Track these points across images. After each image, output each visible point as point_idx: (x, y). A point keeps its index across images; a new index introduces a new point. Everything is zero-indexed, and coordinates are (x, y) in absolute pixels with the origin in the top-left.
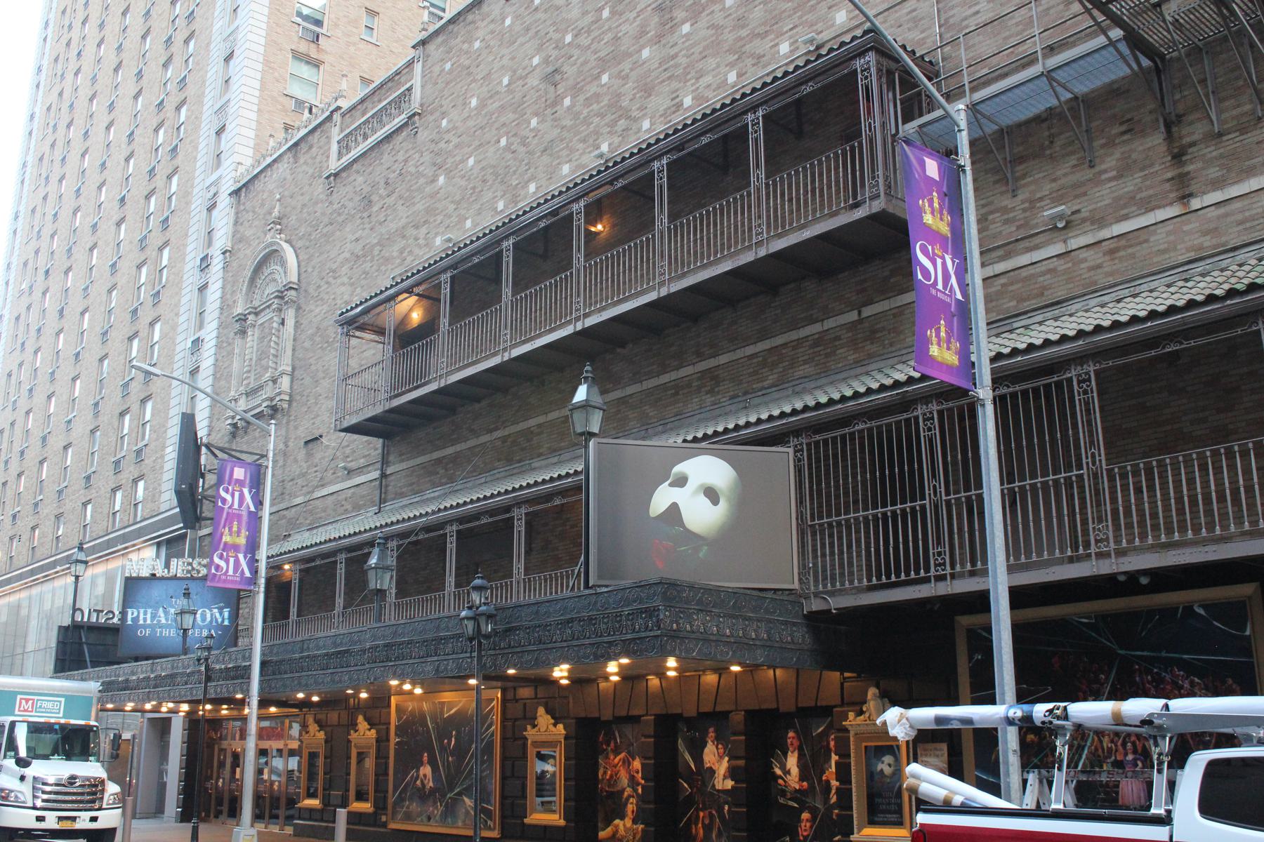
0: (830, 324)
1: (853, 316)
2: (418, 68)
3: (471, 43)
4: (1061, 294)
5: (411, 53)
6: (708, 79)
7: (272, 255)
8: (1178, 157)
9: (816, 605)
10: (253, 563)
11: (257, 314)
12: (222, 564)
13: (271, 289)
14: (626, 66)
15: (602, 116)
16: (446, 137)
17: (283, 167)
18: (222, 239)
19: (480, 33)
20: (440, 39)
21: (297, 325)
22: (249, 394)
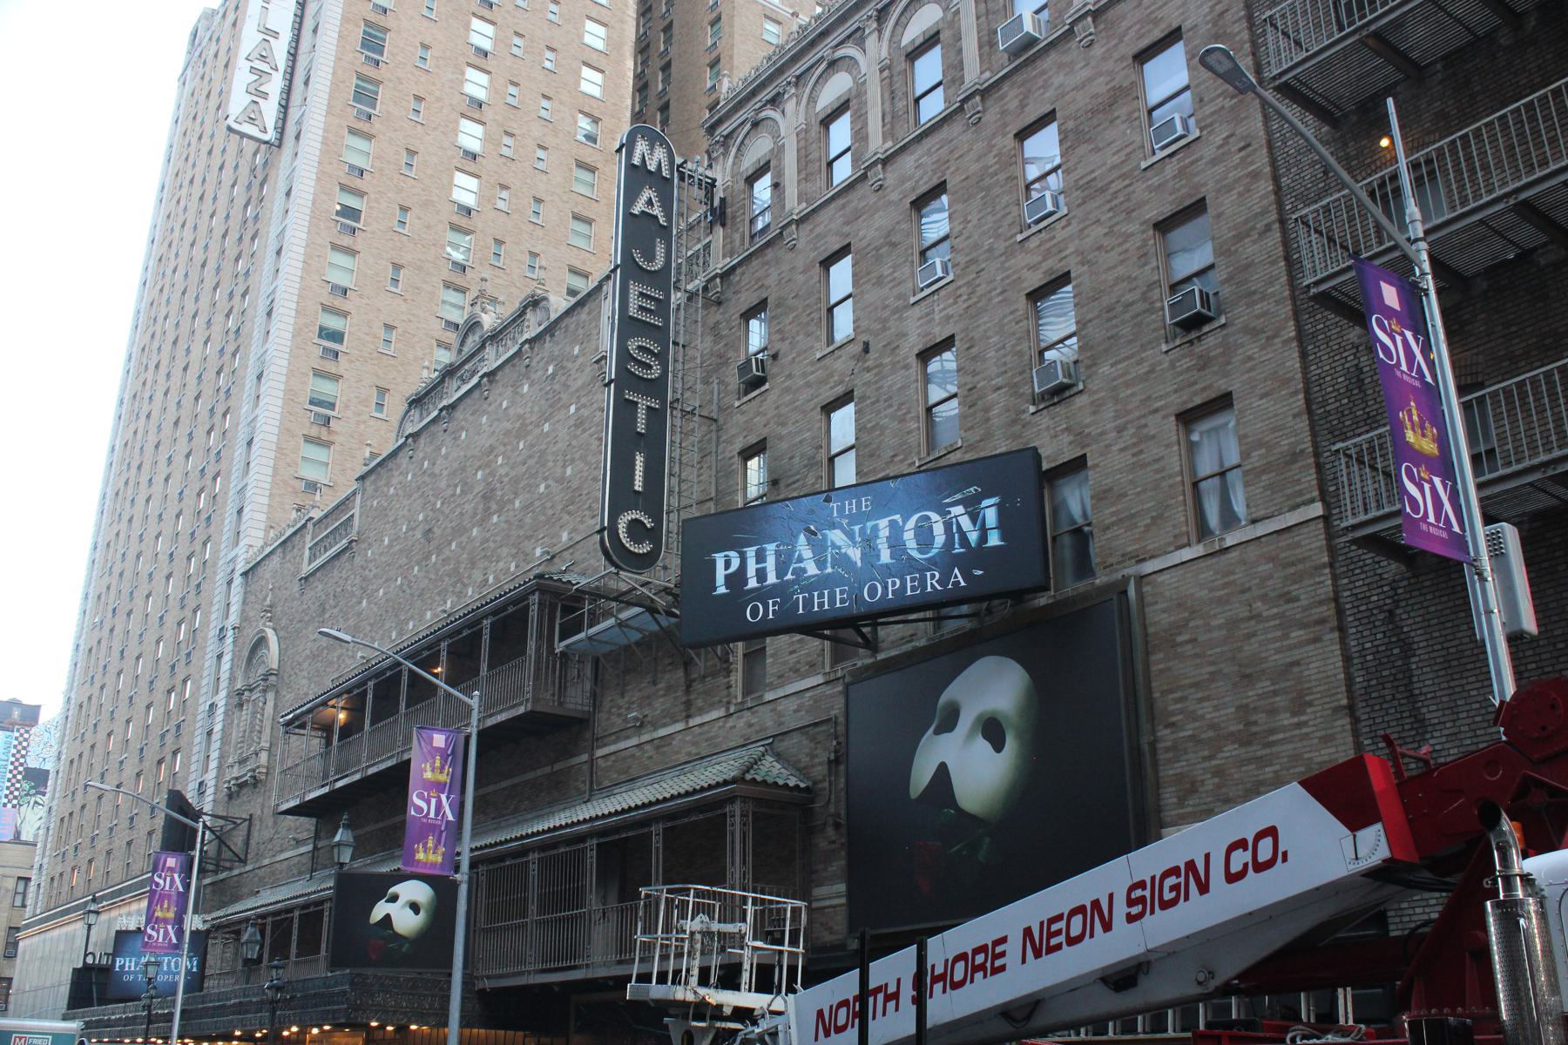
0: (539, 772)
1: (548, 770)
2: (358, 497)
3: (388, 485)
4: (634, 772)
5: (355, 486)
6: (501, 564)
7: (261, 641)
8: (688, 687)
9: (488, 984)
10: (180, 933)
11: (251, 691)
12: (154, 934)
13: (261, 671)
14: (464, 539)
15: (449, 576)
16: (371, 565)
17: (276, 559)
18: (234, 618)
19: (395, 481)
20: (373, 478)
21: (276, 706)
22: (242, 762)
